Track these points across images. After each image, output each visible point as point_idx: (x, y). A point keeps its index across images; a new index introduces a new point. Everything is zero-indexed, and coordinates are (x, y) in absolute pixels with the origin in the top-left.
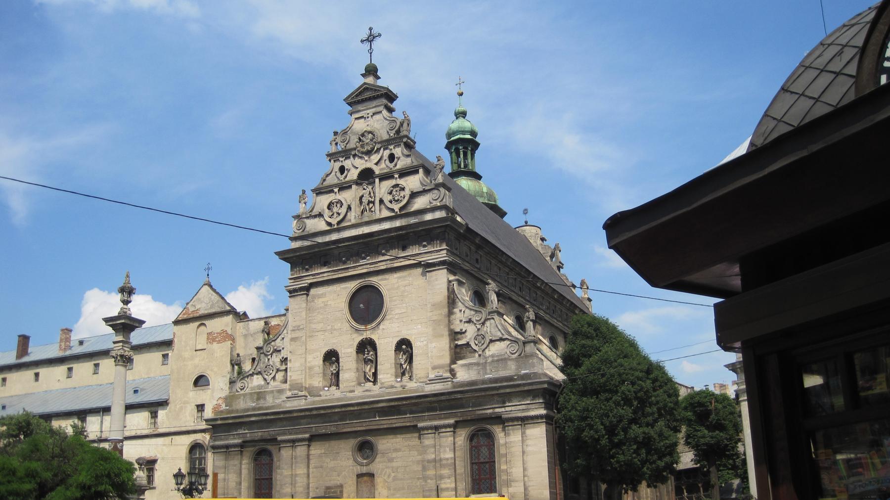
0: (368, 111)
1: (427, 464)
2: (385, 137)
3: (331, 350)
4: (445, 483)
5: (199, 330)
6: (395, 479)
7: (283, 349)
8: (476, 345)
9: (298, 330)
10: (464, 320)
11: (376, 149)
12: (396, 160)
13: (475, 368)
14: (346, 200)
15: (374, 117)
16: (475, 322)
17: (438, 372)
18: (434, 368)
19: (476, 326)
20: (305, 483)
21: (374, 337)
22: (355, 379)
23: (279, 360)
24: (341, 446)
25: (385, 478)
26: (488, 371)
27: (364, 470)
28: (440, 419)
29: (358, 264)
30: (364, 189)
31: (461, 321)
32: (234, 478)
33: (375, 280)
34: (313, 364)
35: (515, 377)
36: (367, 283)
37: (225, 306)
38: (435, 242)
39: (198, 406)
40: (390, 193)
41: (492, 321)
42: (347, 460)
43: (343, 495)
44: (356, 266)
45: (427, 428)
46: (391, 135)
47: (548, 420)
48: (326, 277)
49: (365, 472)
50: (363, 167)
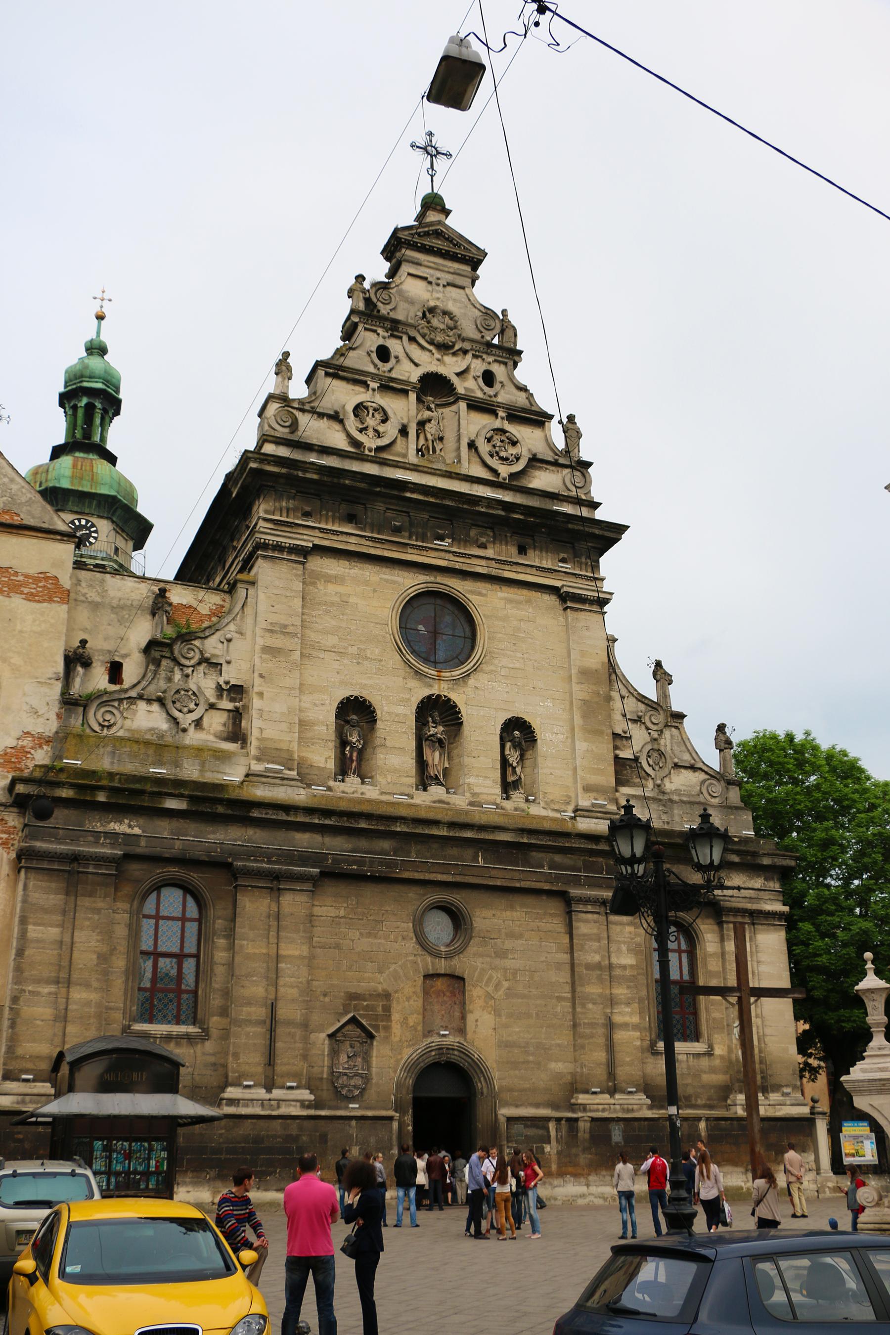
0: (438, 274)
1: (584, 971)
3: (356, 698)
4: (620, 1013)
6: (510, 994)
7: (228, 662)
8: (650, 765)
11: (457, 347)
12: (497, 386)
14: (395, 413)
15: (449, 289)
17: (596, 799)
18: (587, 789)
20: (304, 980)
21: (455, 697)
22: (413, 772)
23: (214, 686)
24: (387, 908)
25: (490, 989)
26: (677, 819)
27: (442, 966)
29: (429, 545)
30: (429, 409)
31: (624, 716)
32: (93, 943)
34: (311, 715)
35: (736, 839)
36: (442, 589)
37: (52, 518)
40: (489, 440)
41: (673, 729)
42: (400, 938)
43: (390, 1016)
44: (426, 547)
45: (587, 901)
46: (489, 338)
47: (790, 923)
48: (353, 544)
49: (443, 972)
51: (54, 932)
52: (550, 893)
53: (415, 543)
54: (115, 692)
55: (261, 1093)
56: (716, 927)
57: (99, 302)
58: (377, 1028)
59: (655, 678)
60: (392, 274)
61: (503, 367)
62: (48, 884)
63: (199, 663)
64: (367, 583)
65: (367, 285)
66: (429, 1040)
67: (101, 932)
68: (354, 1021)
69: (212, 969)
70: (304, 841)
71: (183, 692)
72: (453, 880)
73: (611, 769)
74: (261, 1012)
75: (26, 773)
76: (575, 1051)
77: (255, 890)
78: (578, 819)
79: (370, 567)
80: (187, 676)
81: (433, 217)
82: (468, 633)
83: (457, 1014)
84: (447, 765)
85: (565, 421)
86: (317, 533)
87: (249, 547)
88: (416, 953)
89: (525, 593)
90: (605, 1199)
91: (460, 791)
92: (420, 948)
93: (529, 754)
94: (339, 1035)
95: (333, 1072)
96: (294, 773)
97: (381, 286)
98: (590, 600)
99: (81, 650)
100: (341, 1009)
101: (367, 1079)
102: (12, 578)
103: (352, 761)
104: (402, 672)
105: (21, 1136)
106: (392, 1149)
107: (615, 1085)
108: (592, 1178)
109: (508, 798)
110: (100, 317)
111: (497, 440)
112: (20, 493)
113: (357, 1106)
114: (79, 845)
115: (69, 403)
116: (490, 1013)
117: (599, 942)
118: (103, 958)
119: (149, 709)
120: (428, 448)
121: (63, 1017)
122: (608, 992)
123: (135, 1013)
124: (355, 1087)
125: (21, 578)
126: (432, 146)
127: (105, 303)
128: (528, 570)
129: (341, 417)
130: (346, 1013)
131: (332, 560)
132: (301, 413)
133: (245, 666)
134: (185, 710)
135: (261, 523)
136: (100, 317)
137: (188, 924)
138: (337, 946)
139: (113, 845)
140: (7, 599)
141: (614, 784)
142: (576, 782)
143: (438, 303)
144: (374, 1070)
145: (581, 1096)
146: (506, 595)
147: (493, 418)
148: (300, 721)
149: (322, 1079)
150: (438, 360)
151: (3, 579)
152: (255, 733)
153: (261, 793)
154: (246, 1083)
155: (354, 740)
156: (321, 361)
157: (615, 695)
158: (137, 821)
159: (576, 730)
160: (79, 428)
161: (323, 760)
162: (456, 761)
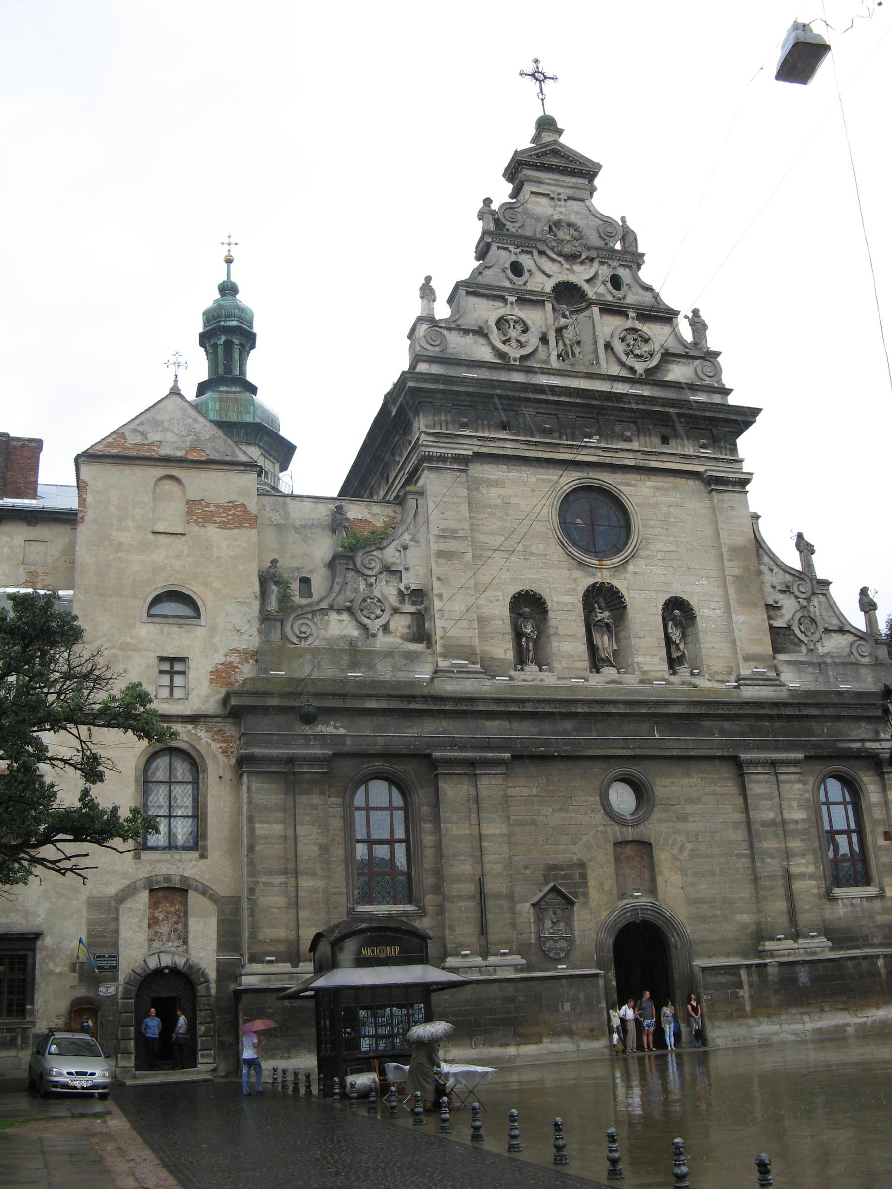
0: (559, 190)
1: (760, 828)
2: (595, 241)
4: (796, 864)
5: (158, 491)
6: (694, 854)
8: (802, 632)
9: (455, 538)
10: (778, 588)
11: (583, 257)
12: (625, 288)
13: (810, 670)
15: (570, 202)
16: (798, 594)
17: (756, 668)
18: (748, 659)
19: (799, 602)
20: (506, 856)
22: (586, 656)
23: (396, 592)
25: (675, 851)
26: (832, 679)
27: (630, 834)
28: (777, 748)
30: (565, 316)
31: (774, 587)
33: (609, 479)
34: (486, 611)
37: (234, 451)
38: (722, 444)
39: (162, 659)
40: (623, 340)
41: (820, 596)
42: (589, 811)
48: (509, 449)
49: (631, 839)
50: (564, 278)
51: (278, 829)
52: (721, 758)
53: (566, 443)
54: (306, 606)
55: (478, 960)
56: (877, 778)
57: (226, 247)
58: (576, 895)
59: (798, 550)
60: (515, 194)
61: (627, 271)
62: (268, 785)
63: (381, 573)
64: (525, 483)
65: (495, 206)
66: (625, 902)
67: (320, 826)
68: (554, 889)
69: (422, 853)
70: (493, 729)
71: (369, 601)
72: (633, 754)
73: (767, 639)
74: (470, 888)
75: (237, 686)
76: (758, 902)
77: (454, 777)
78: (741, 687)
79: (527, 468)
80: (371, 585)
81: (547, 137)
82: (623, 523)
83: (647, 876)
84: (616, 648)
85: (690, 315)
86: (475, 442)
87: (414, 460)
88: (604, 823)
89: (671, 479)
90: (796, 1034)
91: (630, 670)
92: (608, 819)
93: (689, 631)
94: (541, 903)
95: (540, 937)
96: (478, 667)
97: (507, 207)
98: (732, 481)
99: (272, 570)
100: (542, 882)
101: (570, 941)
102: (205, 509)
103: (529, 651)
104: (566, 565)
105: (270, 1010)
106: (600, 1003)
107: (797, 931)
108: (783, 1017)
109: (675, 673)
110: (229, 261)
111: (630, 339)
112: (204, 432)
113: (565, 966)
114: (295, 749)
115: (209, 342)
116: (677, 874)
117: (772, 800)
118: (324, 849)
119: (339, 618)
120: (567, 353)
121: (295, 904)
122: (783, 845)
123: (357, 896)
124: (561, 949)
125: (213, 509)
126: (539, 72)
127: (233, 247)
128: (673, 458)
129: (486, 332)
130: (547, 883)
131: (491, 465)
132: (448, 332)
133: (422, 571)
134: (373, 616)
135: (423, 437)
136: (229, 261)
137: (395, 812)
138: (533, 823)
139: (322, 746)
140: (202, 529)
141: (771, 652)
142: (735, 653)
143: (561, 217)
144: (577, 933)
145: (767, 943)
146: (654, 484)
147: (625, 319)
148: (478, 617)
149: (531, 944)
150: (568, 270)
151: (197, 511)
152: (439, 632)
153: (450, 687)
154: (463, 952)
155: (529, 631)
156: (461, 282)
157: (764, 569)
158: (341, 723)
159: (732, 604)
160: (220, 364)
161: (503, 653)
162: (624, 642)
